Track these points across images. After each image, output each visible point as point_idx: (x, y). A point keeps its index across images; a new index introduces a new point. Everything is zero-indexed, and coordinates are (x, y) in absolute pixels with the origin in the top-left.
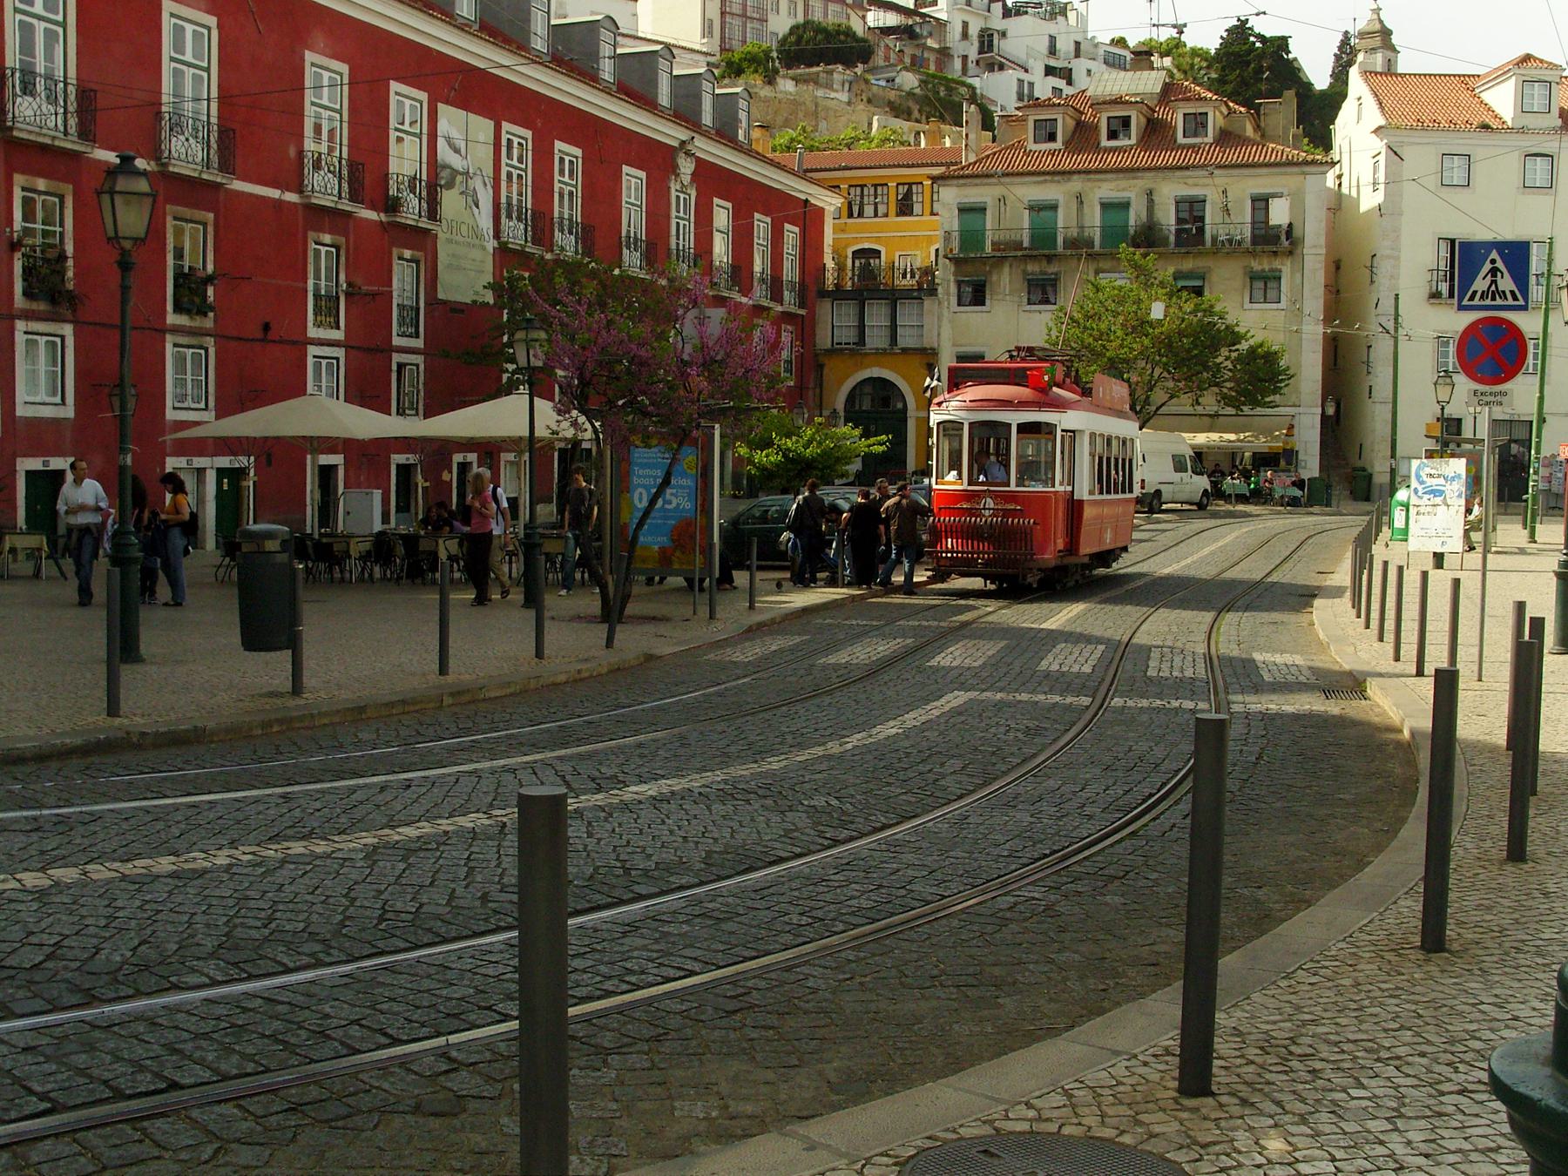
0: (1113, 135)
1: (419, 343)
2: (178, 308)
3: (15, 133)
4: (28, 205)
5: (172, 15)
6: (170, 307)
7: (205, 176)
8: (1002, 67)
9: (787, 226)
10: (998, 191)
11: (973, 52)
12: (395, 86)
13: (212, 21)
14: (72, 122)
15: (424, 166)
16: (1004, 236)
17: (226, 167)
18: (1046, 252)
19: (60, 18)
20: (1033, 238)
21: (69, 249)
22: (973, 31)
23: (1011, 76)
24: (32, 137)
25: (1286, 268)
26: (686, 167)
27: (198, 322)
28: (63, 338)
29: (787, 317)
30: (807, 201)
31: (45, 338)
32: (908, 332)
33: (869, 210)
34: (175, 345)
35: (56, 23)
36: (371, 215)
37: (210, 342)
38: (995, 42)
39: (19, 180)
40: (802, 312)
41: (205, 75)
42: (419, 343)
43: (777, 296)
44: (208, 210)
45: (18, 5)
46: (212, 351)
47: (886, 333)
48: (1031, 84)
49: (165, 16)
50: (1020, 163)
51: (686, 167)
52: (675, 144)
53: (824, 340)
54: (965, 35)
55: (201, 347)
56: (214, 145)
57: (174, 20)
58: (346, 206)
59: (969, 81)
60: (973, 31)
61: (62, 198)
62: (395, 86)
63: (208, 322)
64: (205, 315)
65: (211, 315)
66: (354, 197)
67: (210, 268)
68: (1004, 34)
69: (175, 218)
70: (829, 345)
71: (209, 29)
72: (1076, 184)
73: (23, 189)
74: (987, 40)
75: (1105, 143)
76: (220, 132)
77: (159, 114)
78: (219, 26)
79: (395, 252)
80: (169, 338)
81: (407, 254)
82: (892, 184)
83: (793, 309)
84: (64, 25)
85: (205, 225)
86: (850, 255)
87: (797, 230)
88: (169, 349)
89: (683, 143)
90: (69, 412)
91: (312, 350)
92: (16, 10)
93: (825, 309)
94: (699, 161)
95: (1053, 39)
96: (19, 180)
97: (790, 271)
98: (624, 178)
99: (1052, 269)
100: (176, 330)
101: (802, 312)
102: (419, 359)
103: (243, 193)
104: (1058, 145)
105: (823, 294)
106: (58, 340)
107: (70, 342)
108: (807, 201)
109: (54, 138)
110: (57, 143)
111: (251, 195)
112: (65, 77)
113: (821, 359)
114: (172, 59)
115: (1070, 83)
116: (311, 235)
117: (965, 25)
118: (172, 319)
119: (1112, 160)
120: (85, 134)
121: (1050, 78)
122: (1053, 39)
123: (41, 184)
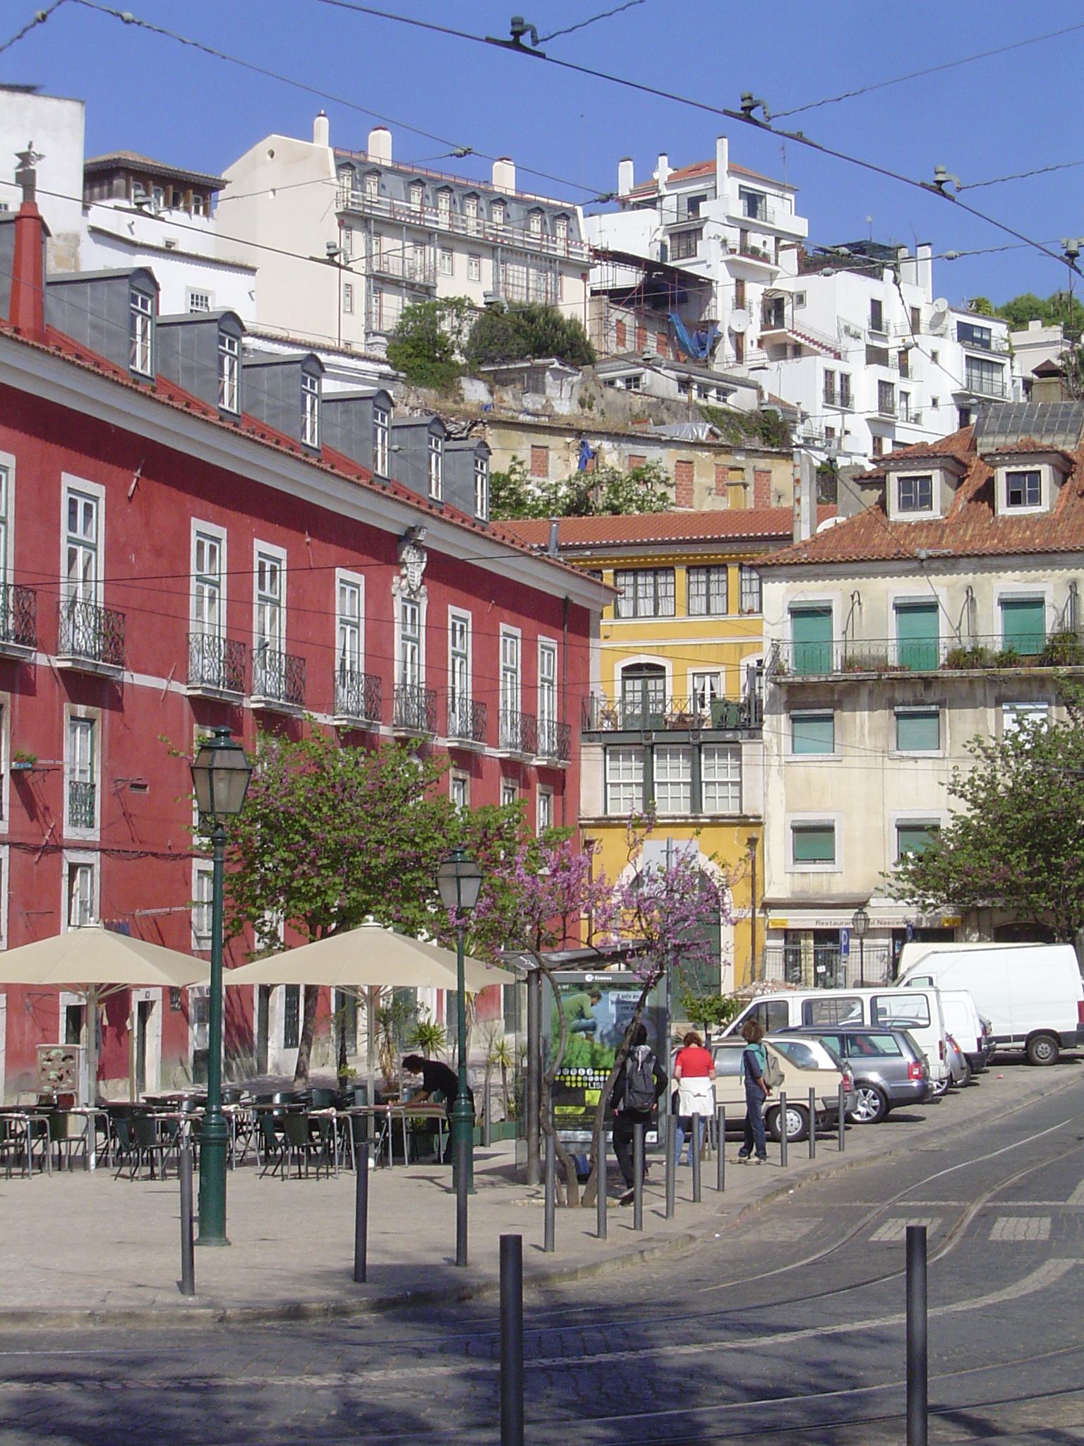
0: (1015, 499)
1: (94, 835)
8: (798, 350)
10: (848, 585)
11: (753, 331)
16: (855, 650)
18: (925, 673)
20: (902, 653)
22: (754, 292)
23: (812, 369)
29: (547, 774)
30: (567, 600)
32: (719, 791)
38: (788, 310)
42: (94, 835)
48: (845, 378)
50: (880, 542)
51: (414, 566)
53: (590, 803)
54: (740, 302)
59: (753, 376)
60: (754, 292)
68: (801, 299)
70: (600, 814)
74: (774, 308)
75: (1004, 509)
81: (81, 710)
86: (618, 674)
95: (876, 306)
98: (338, 585)
102: (94, 858)
105: (591, 735)
108: (567, 600)
115: (904, 372)
117: (740, 284)
119: (1016, 538)
121: (875, 367)
122: (876, 306)
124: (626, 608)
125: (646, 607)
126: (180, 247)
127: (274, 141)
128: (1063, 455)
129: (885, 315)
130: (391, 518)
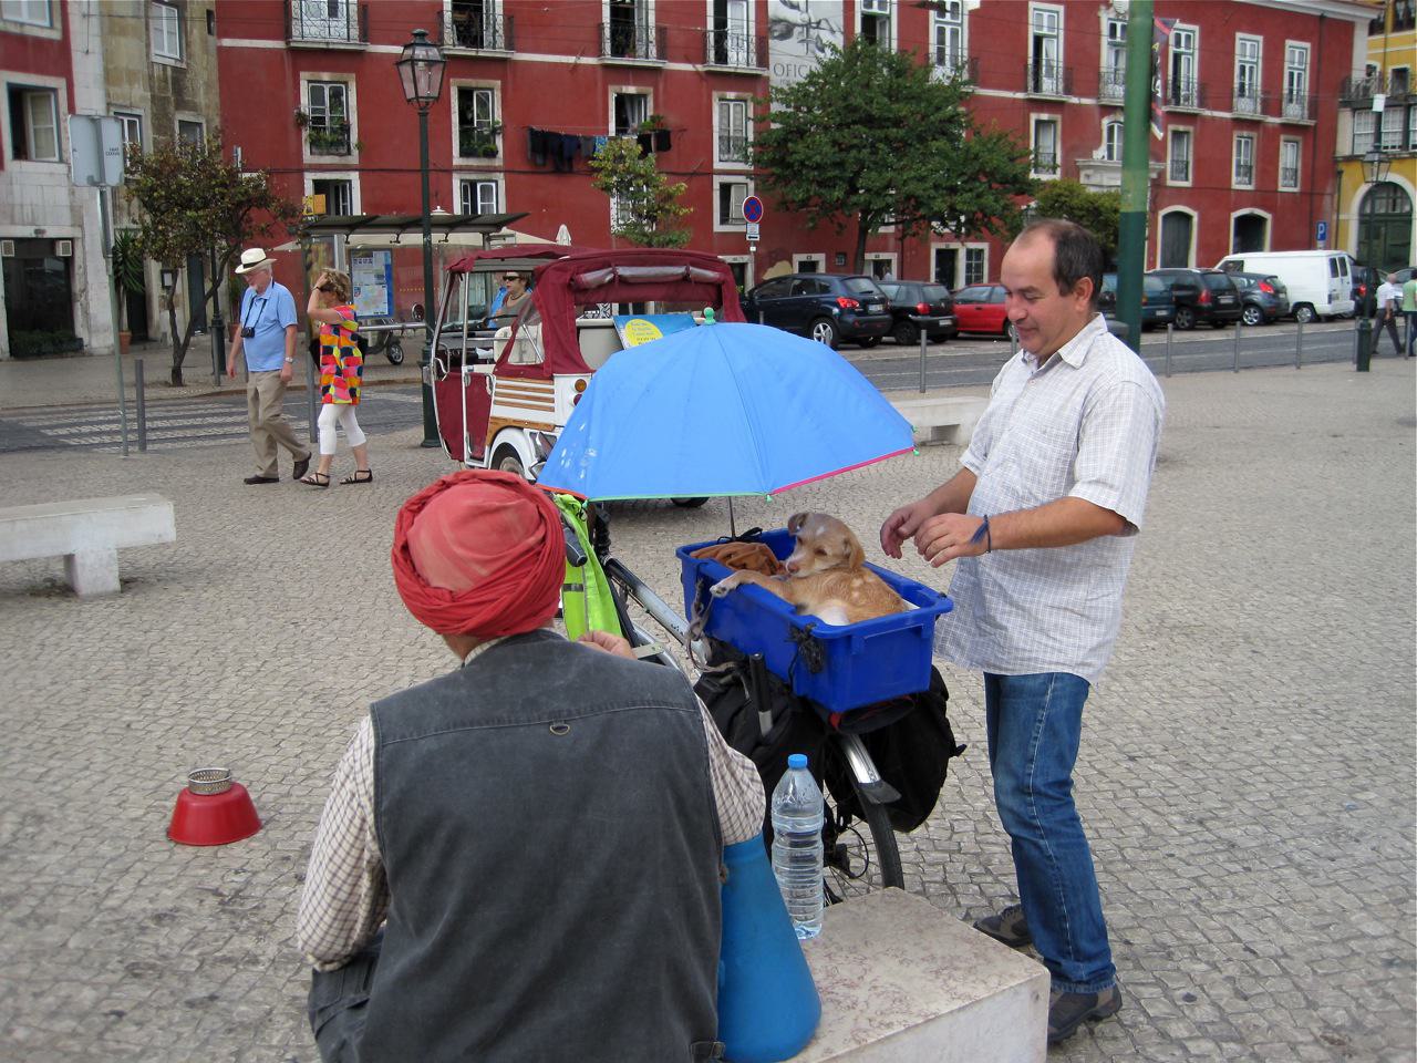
2: (463, 154)
4: (316, 96)
15: (752, 25)
21: (354, 120)
24: (342, 47)
27: (484, 162)
36: (688, 67)
37: (500, 177)
39: (304, 76)
46: (502, 184)
61: (346, 83)
73: (309, 81)
96: (304, 76)
100: (461, 169)
110: (331, 47)
113: (1342, 167)
118: (457, 161)
123: (326, 76)
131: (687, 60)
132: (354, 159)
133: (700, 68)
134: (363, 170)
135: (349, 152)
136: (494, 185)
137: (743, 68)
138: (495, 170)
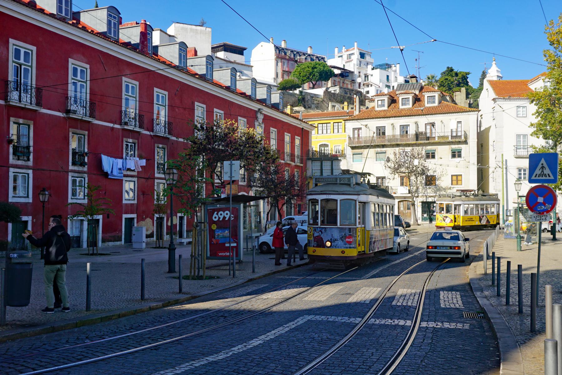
2: (74, 164)
3: (11, 103)
5: (72, 64)
6: (70, 164)
7: (83, 119)
9: (296, 137)
12: (156, 89)
13: (88, 66)
14: (34, 100)
15: (167, 117)
17: (91, 116)
19: (30, 64)
25: (463, 147)
26: (260, 117)
27: (81, 169)
28: (28, 174)
29: (297, 166)
31: (21, 174)
33: (325, 131)
34: (72, 177)
35: (29, 66)
36: (147, 133)
39: (12, 119)
40: (302, 165)
41: (85, 84)
43: (293, 160)
44: (86, 130)
45: (14, 60)
46: (86, 179)
47: (319, 171)
49: (70, 64)
50: (372, 114)
51: (260, 117)
52: (256, 109)
55: (82, 177)
56: (88, 109)
57: (73, 66)
58: (137, 129)
61: (29, 126)
62: (156, 89)
63: (86, 169)
64: (84, 166)
65: (86, 166)
66: (140, 127)
67: (86, 150)
69: (73, 133)
71: (87, 69)
72: (392, 120)
76: (91, 104)
77: (67, 98)
78: (90, 68)
79: (156, 145)
80: (70, 174)
81: (161, 146)
82: (332, 123)
83: (298, 164)
84: (31, 67)
85: (84, 135)
87: (299, 138)
88: (70, 179)
89: (259, 109)
90: (30, 200)
91: (12, 170)
92: (13, 62)
93: (309, 163)
94: (265, 115)
95: (388, 76)
96: (12, 119)
97: (297, 152)
99: (384, 149)
101: (302, 165)
103: (99, 125)
104: (386, 108)
106: (27, 175)
107: (31, 176)
109: (25, 105)
110: (27, 107)
111: (102, 125)
112: (31, 84)
114: (72, 79)
116: (125, 139)
118: (71, 167)
119: (403, 113)
120: (38, 104)
122: (388, 76)
123: (21, 121)
124: (320, 132)
125: (325, 131)
126: (237, 62)
127: (262, 43)
128: (415, 94)
129: (390, 78)
130: (255, 106)
131: (148, 130)
132: (31, 163)
133: (152, 134)
134: (34, 169)
135: (28, 160)
136: (83, 179)
137: (162, 134)
138: (85, 173)
